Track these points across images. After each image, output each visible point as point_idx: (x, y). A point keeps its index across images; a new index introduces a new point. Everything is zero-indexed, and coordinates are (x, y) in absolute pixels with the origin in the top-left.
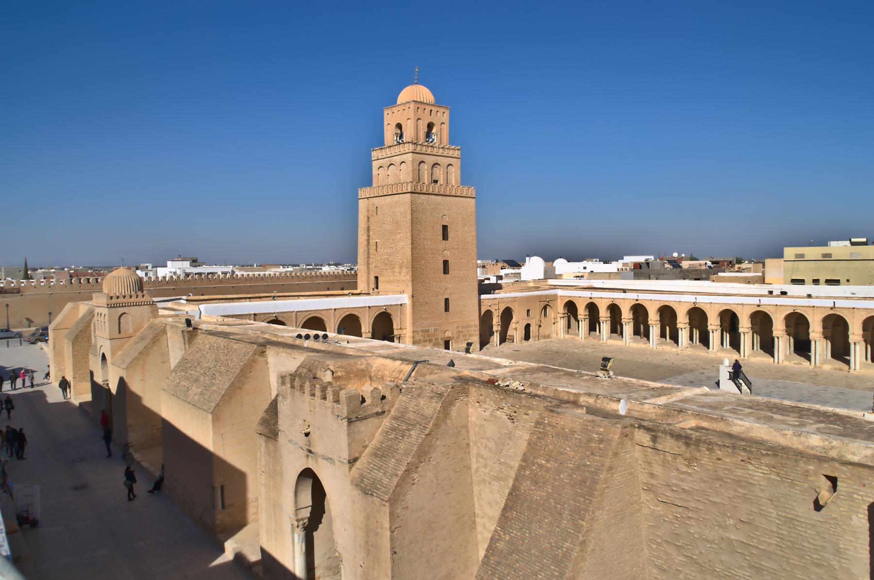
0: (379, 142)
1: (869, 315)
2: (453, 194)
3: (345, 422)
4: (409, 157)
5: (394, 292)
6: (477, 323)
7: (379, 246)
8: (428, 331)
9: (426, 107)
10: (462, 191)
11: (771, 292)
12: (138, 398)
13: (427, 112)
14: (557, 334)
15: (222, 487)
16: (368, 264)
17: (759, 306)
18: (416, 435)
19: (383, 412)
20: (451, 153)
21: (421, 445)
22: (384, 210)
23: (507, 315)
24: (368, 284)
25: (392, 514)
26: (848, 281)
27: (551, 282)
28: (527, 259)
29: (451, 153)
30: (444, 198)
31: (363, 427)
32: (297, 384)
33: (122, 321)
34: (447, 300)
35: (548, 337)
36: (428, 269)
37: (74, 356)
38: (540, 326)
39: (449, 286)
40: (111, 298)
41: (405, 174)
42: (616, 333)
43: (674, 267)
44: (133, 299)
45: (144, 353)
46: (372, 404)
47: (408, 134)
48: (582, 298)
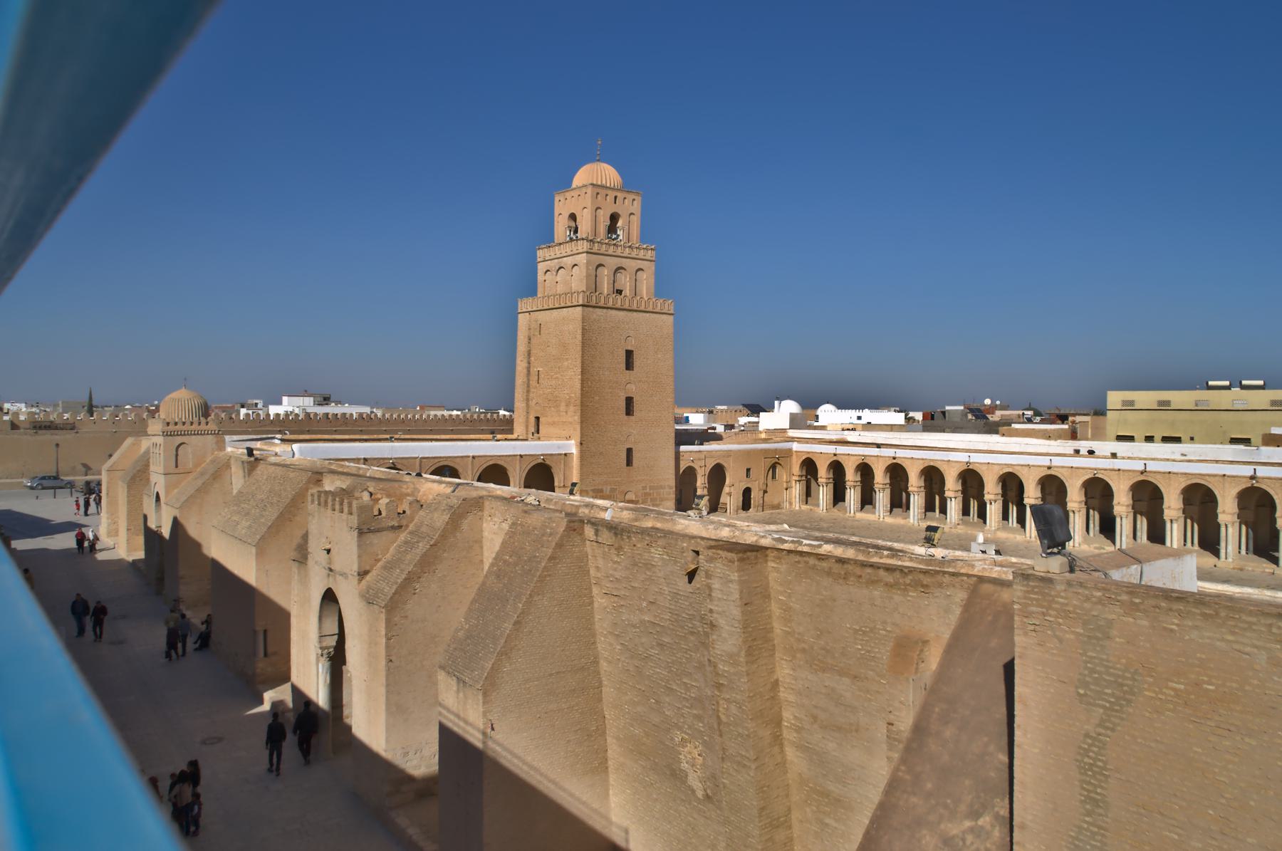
0: (548, 239)
1: (1189, 482)
2: (642, 308)
3: (356, 533)
4: (582, 259)
5: (559, 438)
6: (672, 483)
7: (542, 376)
8: (601, 491)
9: (609, 192)
10: (655, 305)
11: (1077, 452)
12: (198, 546)
13: (610, 198)
14: (791, 504)
15: (265, 631)
16: (528, 400)
17: (1049, 468)
18: (422, 547)
19: (400, 527)
20: (642, 254)
21: (424, 555)
22: (549, 328)
23: (717, 475)
24: (527, 427)
25: (388, 621)
26: (1192, 439)
27: (792, 433)
28: (776, 403)
29: (642, 254)
30: (629, 314)
31: (376, 540)
32: (322, 500)
33: (180, 452)
34: (629, 451)
35: (778, 507)
36: (604, 405)
37: (129, 502)
38: (765, 492)
39: (632, 431)
40: (168, 424)
41: (577, 280)
42: (900, 506)
43: (977, 417)
44: (195, 427)
45: (202, 490)
46: (388, 517)
47: (585, 227)
48: (851, 457)
